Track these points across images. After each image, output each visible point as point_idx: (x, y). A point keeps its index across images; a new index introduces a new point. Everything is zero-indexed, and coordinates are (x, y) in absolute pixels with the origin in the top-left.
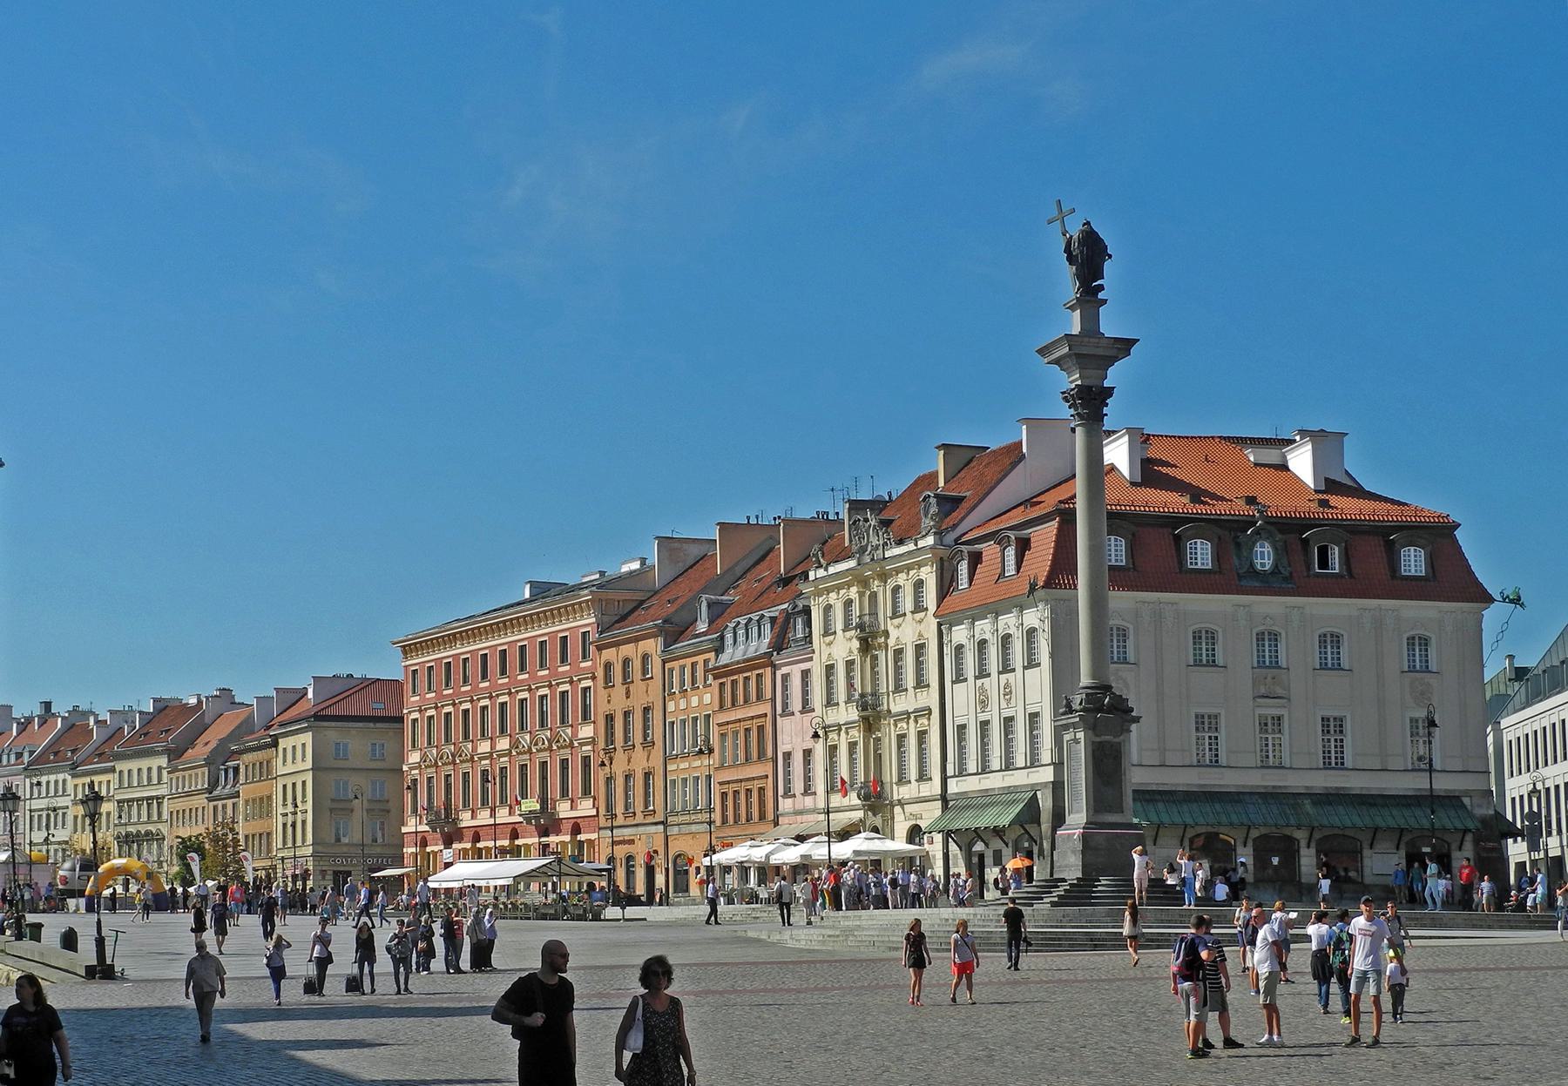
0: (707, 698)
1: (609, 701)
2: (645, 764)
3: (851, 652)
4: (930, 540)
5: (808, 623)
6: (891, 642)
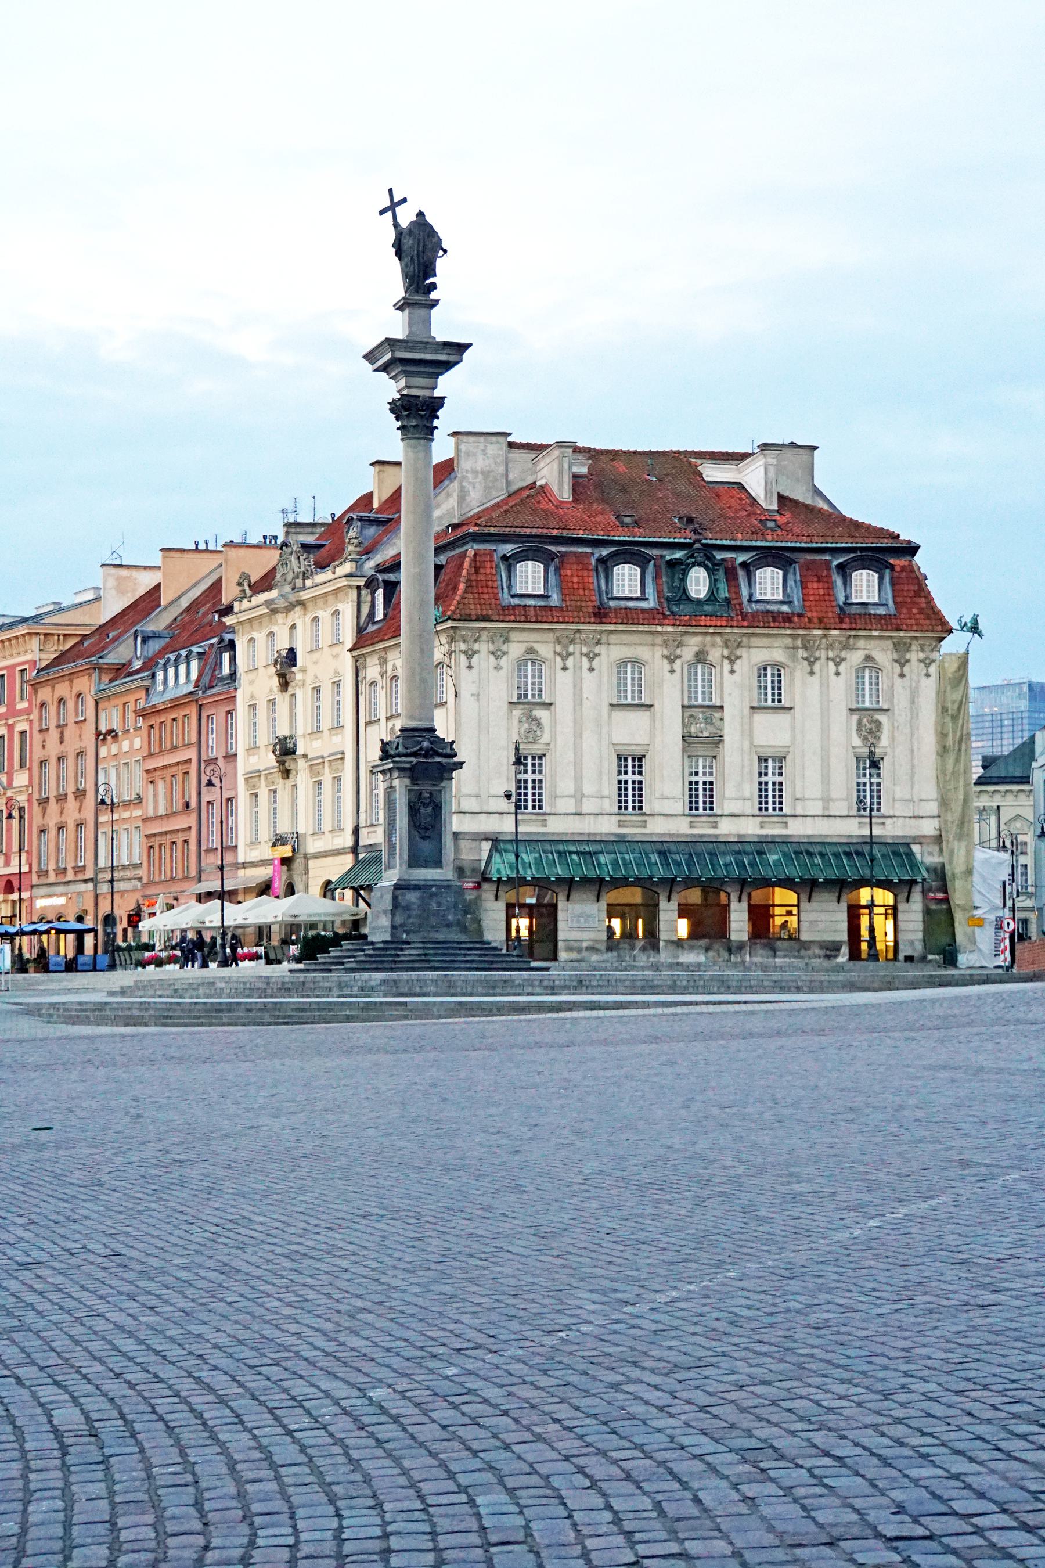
0: (138, 743)
1: (44, 747)
2: (76, 815)
3: (271, 690)
4: (348, 568)
5: (233, 659)
6: (309, 679)
